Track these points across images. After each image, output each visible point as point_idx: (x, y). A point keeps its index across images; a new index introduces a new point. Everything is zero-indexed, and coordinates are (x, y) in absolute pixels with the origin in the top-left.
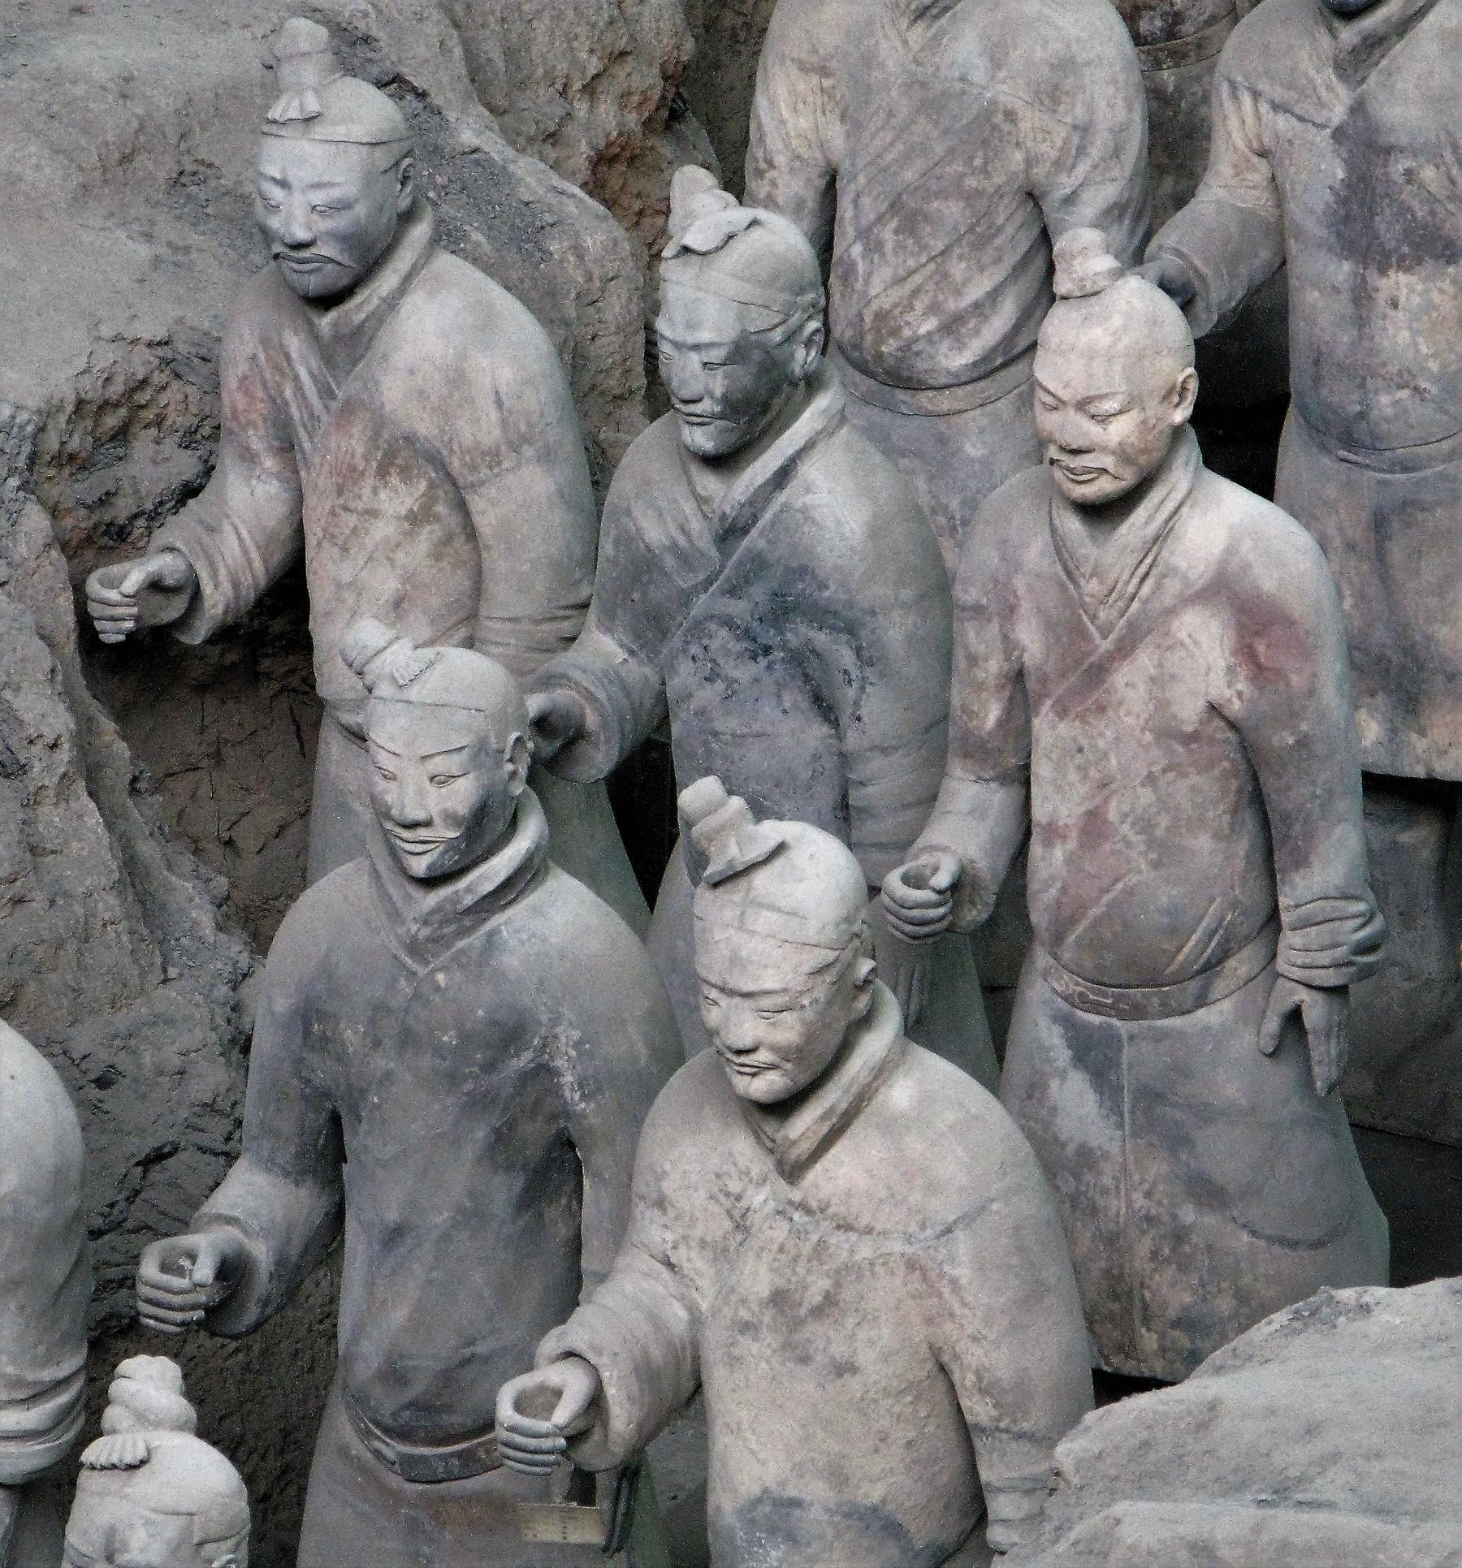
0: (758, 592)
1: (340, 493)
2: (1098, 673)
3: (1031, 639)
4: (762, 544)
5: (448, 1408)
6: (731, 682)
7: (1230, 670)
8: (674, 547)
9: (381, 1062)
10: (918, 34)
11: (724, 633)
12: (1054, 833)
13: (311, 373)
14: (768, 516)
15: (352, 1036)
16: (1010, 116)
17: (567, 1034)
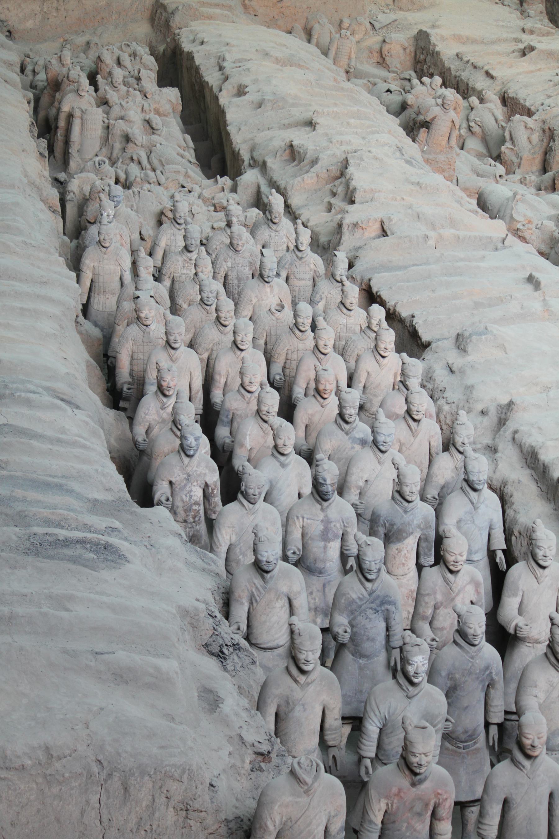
0: (378, 602)
1: (268, 605)
2: (453, 599)
3: (439, 597)
4: (379, 593)
5: (474, 735)
6: (370, 619)
7: (474, 594)
8: (359, 598)
9: (463, 679)
10: (253, 517)
11: (370, 610)
12: (442, 629)
13: (261, 586)
14: (379, 588)
15: (457, 676)
16: (267, 529)
17: (495, 666)
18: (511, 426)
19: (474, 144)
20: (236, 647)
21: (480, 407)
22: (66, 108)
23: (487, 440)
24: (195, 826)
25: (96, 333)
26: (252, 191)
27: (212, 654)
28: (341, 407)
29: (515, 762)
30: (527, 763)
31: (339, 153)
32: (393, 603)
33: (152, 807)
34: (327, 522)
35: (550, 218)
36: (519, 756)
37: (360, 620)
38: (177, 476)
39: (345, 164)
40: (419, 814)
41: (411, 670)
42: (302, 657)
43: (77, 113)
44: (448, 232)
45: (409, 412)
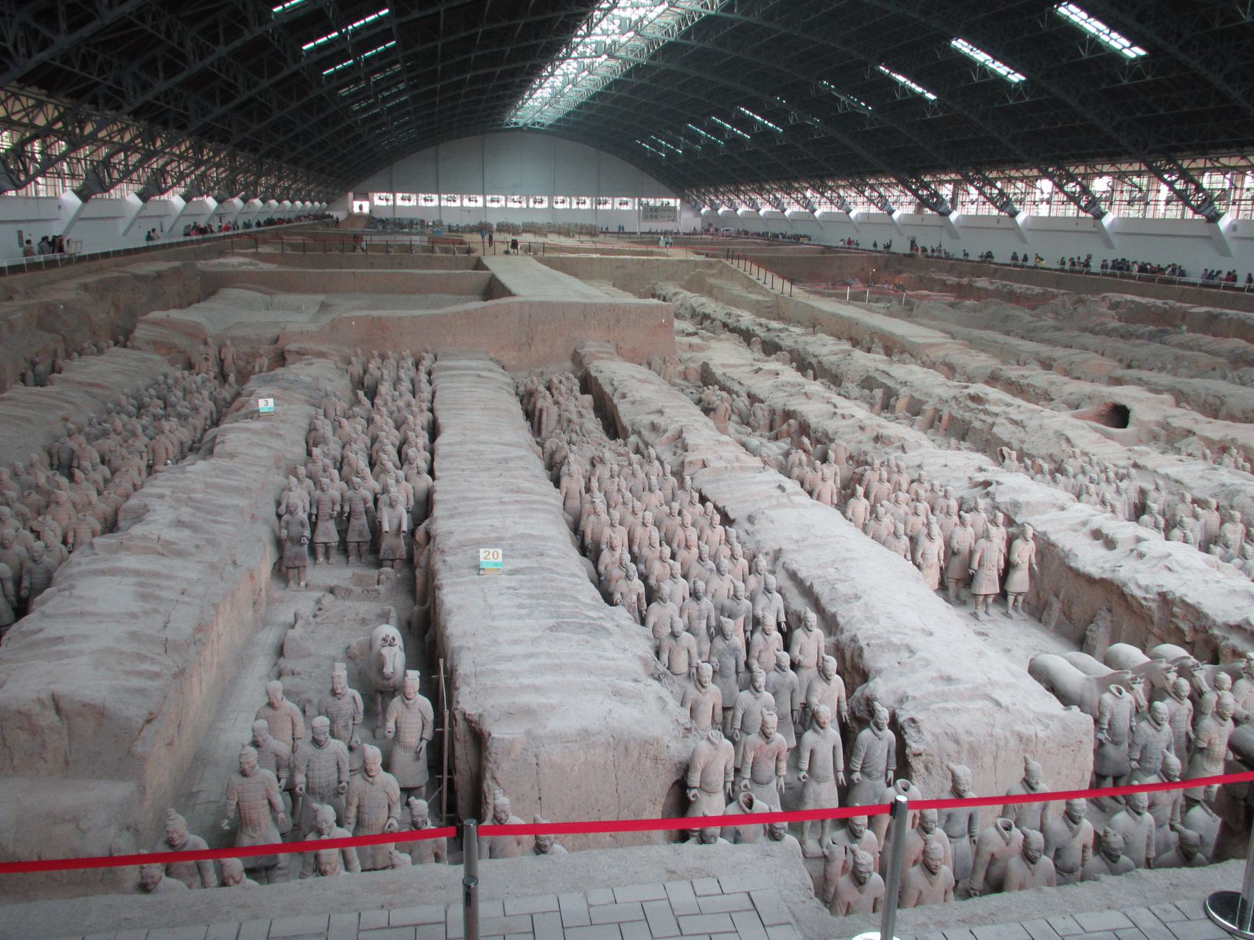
18: (782, 560)
19: (734, 418)
20: (665, 674)
21: (764, 551)
22: (538, 406)
23: (770, 568)
24: (660, 767)
25: (571, 519)
26: (634, 446)
27: (654, 678)
28: (700, 553)
29: (815, 731)
30: (821, 731)
31: (677, 426)
32: (739, 651)
33: (639, 759)
34: (700, 610)
35: (779, 454)
36: (818, 728)
37: (724, 659)
38: (625, 590)
39: (681, 431)
40: (771, 758)
41: (757, 685)
42: (703, 680)
43: (545, 408)
44: (736, 465)
45: (732, 555)
